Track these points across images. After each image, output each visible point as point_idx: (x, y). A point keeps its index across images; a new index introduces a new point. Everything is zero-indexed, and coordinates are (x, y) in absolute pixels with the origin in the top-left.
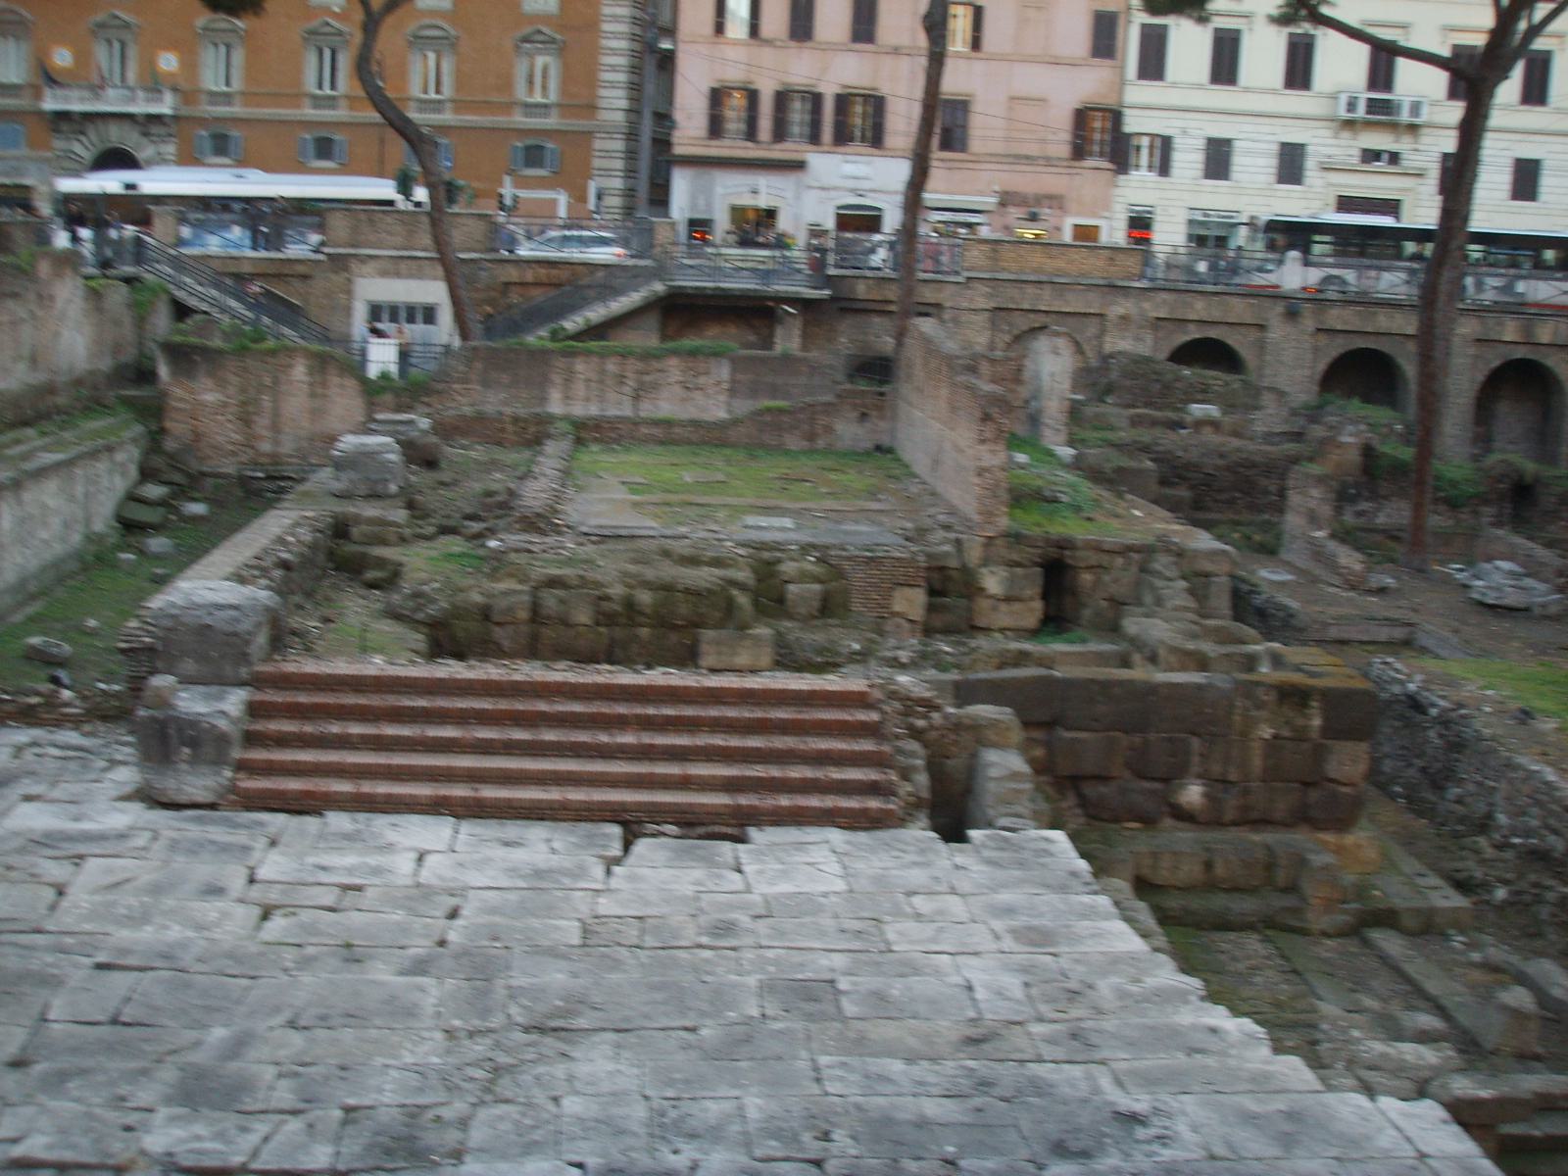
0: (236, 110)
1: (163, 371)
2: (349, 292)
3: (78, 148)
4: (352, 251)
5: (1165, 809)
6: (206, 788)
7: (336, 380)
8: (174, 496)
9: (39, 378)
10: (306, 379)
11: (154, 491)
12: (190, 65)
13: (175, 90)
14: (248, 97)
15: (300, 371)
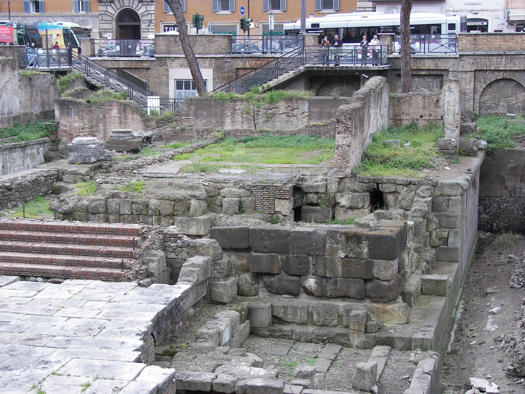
1: (57, 113)
3: (110, 9)
4: (166, 56)
5: (302, 289)
10: (116, 115)
15: (115, 112)
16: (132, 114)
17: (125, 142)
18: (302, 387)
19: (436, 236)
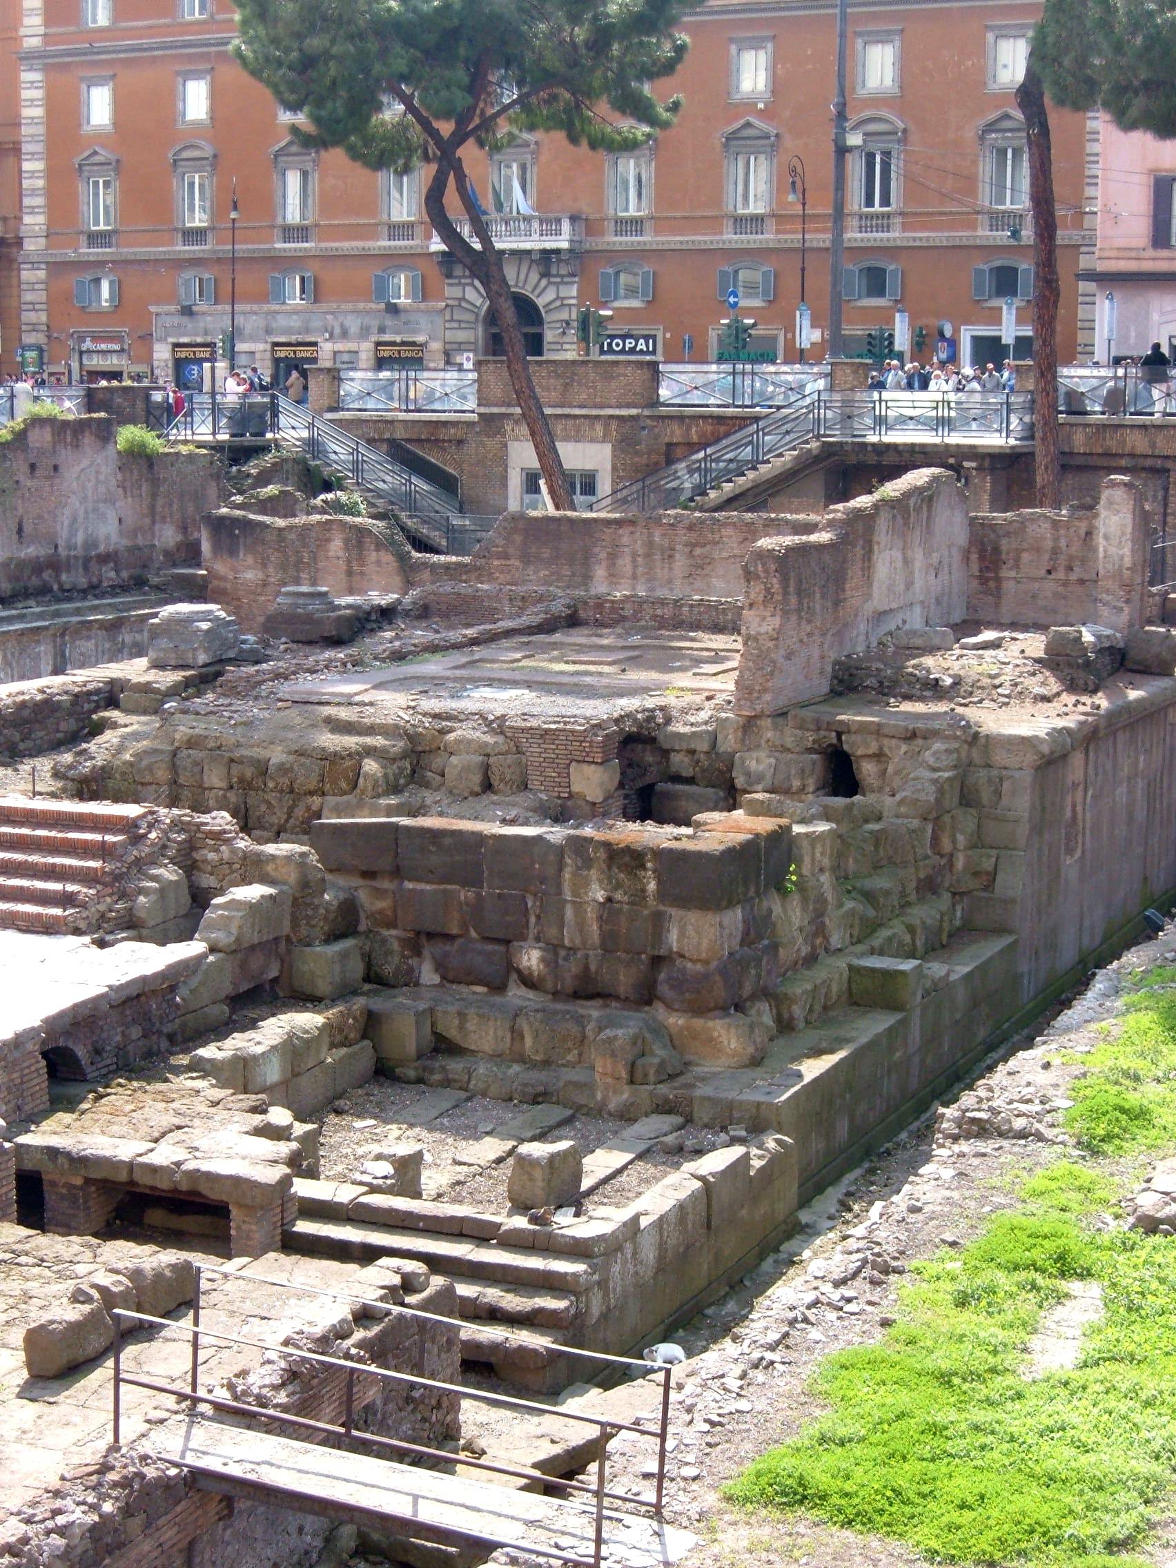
1: (206, 547)
3: (471, 294)
4: (503, 410)
5: (514, 976)
10: (341, 554)
13: (573, 219)
15: (336, 546)
17: (309, 619)
18: (365, 1189)
19: (967, 867)
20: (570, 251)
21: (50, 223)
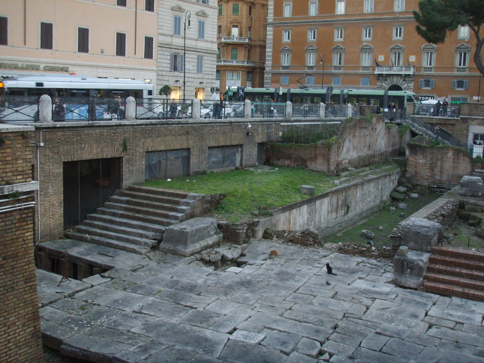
0: (433, 72)
1: (407, 152)
2: (468, 130)
3: (384, 84)
4: (469, 117)
6: (414, 283)
7: (462, 158)
8: (408, 191)
9: (370, 153)
10: (451, 157)
11: (402, 189)
12: (419, 59)
13: (414, 67)
14: (437, 68)
15: (450, 154)
16: (464, 156)
20: (413, 75)
21: (273, 63)
